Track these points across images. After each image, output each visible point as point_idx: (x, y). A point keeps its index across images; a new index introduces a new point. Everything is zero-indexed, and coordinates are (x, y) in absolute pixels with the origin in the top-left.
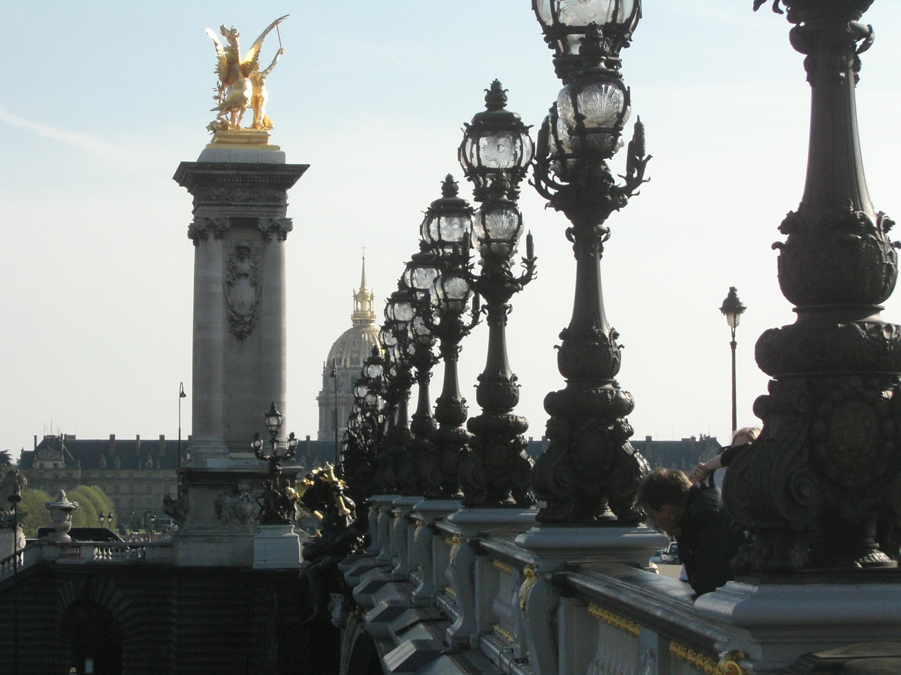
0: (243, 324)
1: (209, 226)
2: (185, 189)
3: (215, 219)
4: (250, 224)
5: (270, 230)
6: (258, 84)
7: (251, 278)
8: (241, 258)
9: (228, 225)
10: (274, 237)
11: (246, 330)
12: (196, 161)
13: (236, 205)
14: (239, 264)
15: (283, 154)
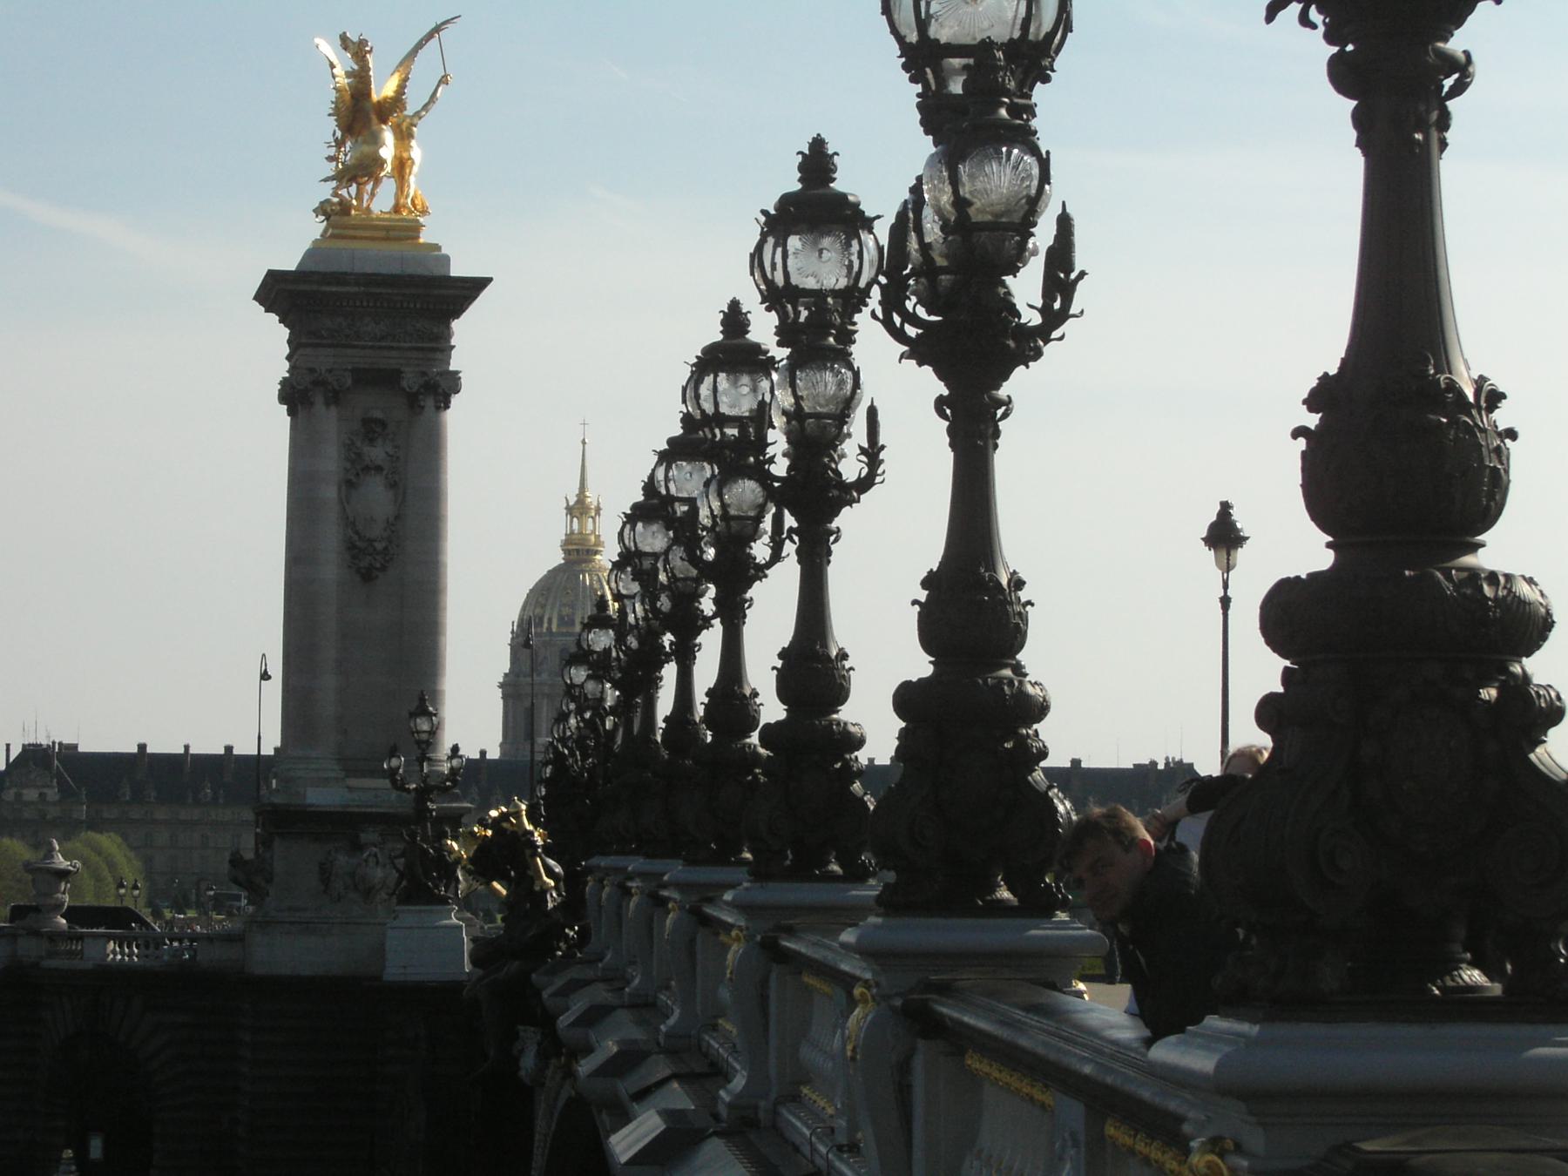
0: (370, 555)
1: (316, 383)
2: (274, 318)
3: (327, 370)
4: (387, 379)
5: (422, 390)
6: (404, 136)
7: (387, 474)
8: (372, 441)
9: (349, 382)
10: (429, 403)
11: (378, 565)
12: (294, 269)
13: (364, 348)
14: (366, 449)
15: (446, 259)
